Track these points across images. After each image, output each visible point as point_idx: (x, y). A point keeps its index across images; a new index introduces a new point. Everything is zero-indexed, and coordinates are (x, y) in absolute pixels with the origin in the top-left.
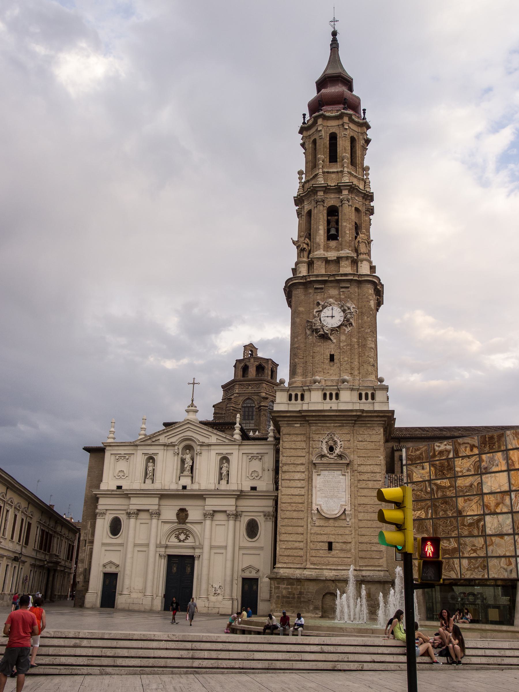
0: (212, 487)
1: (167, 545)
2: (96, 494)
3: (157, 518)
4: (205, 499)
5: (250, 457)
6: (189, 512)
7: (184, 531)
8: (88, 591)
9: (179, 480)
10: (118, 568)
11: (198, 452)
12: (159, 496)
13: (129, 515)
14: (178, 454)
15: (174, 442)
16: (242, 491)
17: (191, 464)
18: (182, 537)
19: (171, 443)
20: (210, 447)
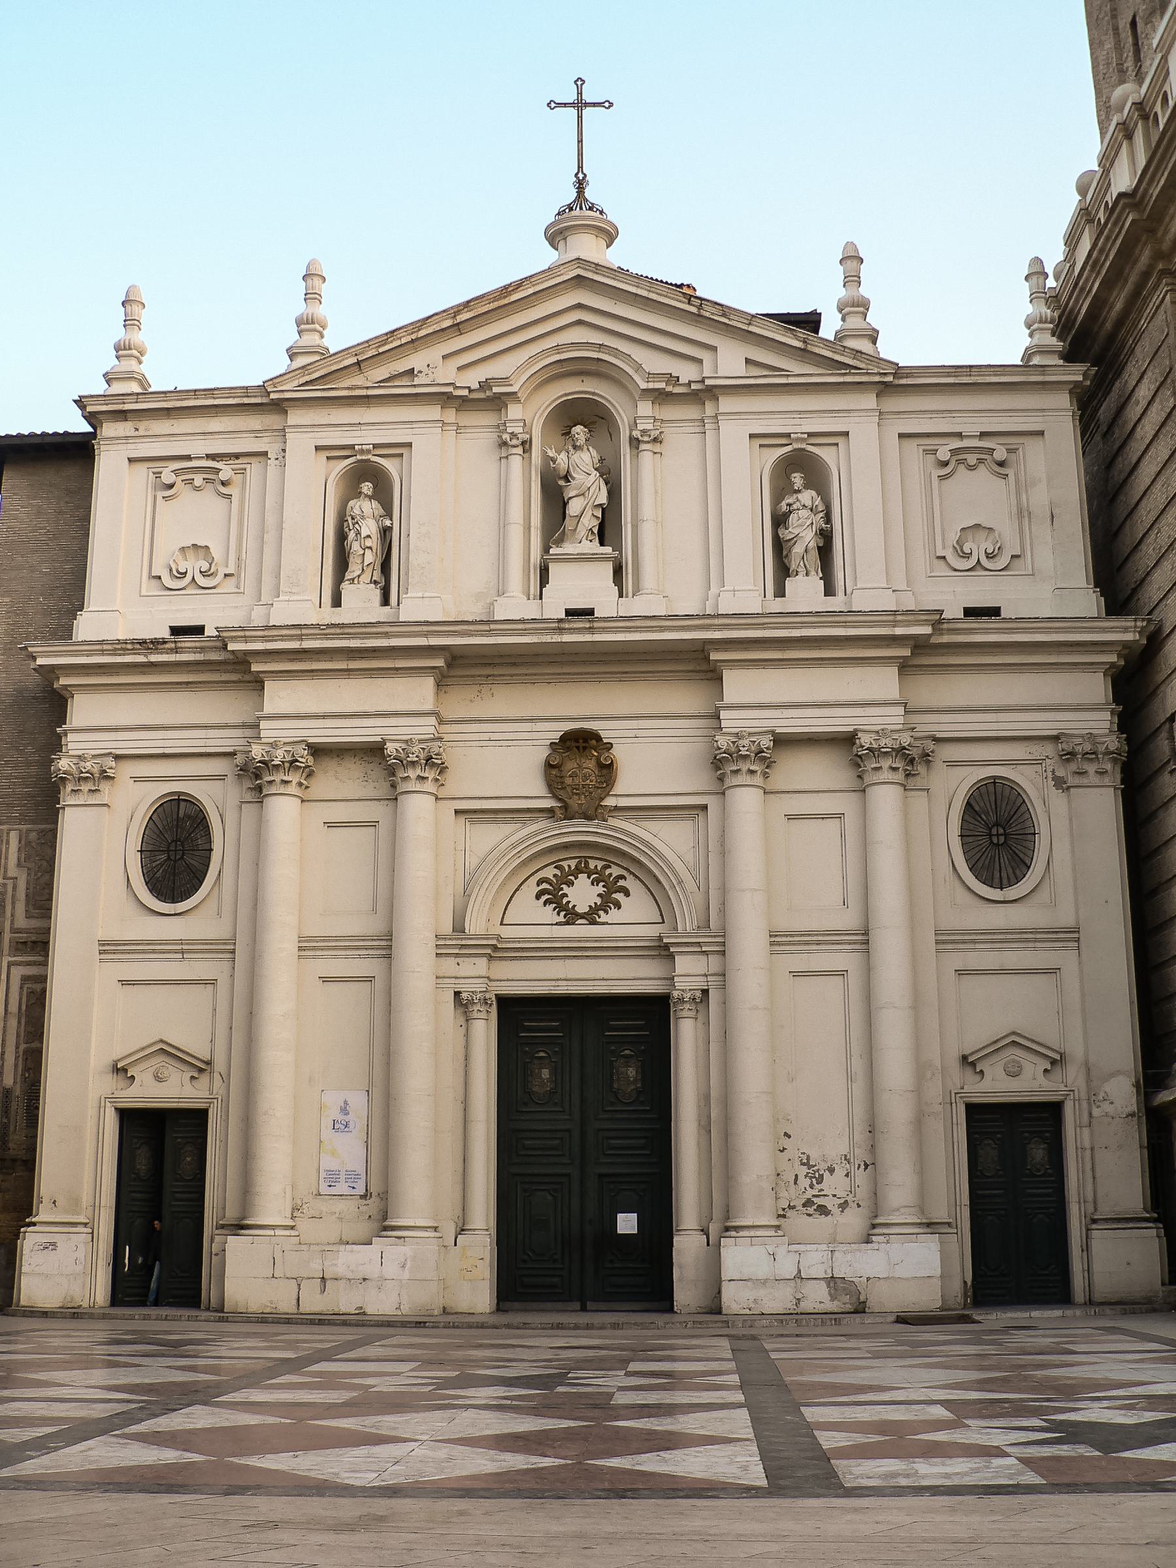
0: (752, 603)
1: (499, 938)
2: (51, 672)
3: (429, 786)
4: (713, 676)
5: (943, 454)
6: (620, 753)
7: (592, 864)
8: (30, 1215)
9: (544, 580)
10: (204, 1079)
11: (644, 432)
12: (440, 663)
13: (258, 776)
14: (526, 445)
15: (504, 381)
16: (938, 620)
17: (603, 499)
18: (583, 894)
19: (485, 385)
20: (709, 409)
